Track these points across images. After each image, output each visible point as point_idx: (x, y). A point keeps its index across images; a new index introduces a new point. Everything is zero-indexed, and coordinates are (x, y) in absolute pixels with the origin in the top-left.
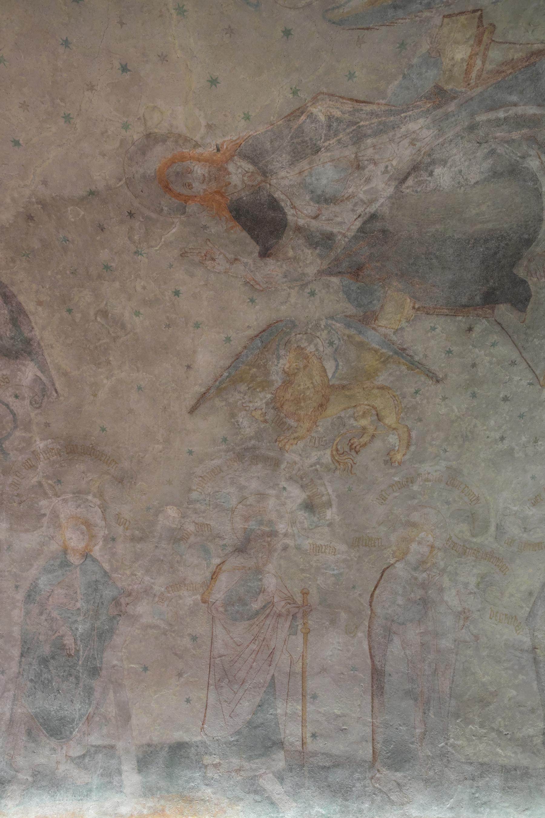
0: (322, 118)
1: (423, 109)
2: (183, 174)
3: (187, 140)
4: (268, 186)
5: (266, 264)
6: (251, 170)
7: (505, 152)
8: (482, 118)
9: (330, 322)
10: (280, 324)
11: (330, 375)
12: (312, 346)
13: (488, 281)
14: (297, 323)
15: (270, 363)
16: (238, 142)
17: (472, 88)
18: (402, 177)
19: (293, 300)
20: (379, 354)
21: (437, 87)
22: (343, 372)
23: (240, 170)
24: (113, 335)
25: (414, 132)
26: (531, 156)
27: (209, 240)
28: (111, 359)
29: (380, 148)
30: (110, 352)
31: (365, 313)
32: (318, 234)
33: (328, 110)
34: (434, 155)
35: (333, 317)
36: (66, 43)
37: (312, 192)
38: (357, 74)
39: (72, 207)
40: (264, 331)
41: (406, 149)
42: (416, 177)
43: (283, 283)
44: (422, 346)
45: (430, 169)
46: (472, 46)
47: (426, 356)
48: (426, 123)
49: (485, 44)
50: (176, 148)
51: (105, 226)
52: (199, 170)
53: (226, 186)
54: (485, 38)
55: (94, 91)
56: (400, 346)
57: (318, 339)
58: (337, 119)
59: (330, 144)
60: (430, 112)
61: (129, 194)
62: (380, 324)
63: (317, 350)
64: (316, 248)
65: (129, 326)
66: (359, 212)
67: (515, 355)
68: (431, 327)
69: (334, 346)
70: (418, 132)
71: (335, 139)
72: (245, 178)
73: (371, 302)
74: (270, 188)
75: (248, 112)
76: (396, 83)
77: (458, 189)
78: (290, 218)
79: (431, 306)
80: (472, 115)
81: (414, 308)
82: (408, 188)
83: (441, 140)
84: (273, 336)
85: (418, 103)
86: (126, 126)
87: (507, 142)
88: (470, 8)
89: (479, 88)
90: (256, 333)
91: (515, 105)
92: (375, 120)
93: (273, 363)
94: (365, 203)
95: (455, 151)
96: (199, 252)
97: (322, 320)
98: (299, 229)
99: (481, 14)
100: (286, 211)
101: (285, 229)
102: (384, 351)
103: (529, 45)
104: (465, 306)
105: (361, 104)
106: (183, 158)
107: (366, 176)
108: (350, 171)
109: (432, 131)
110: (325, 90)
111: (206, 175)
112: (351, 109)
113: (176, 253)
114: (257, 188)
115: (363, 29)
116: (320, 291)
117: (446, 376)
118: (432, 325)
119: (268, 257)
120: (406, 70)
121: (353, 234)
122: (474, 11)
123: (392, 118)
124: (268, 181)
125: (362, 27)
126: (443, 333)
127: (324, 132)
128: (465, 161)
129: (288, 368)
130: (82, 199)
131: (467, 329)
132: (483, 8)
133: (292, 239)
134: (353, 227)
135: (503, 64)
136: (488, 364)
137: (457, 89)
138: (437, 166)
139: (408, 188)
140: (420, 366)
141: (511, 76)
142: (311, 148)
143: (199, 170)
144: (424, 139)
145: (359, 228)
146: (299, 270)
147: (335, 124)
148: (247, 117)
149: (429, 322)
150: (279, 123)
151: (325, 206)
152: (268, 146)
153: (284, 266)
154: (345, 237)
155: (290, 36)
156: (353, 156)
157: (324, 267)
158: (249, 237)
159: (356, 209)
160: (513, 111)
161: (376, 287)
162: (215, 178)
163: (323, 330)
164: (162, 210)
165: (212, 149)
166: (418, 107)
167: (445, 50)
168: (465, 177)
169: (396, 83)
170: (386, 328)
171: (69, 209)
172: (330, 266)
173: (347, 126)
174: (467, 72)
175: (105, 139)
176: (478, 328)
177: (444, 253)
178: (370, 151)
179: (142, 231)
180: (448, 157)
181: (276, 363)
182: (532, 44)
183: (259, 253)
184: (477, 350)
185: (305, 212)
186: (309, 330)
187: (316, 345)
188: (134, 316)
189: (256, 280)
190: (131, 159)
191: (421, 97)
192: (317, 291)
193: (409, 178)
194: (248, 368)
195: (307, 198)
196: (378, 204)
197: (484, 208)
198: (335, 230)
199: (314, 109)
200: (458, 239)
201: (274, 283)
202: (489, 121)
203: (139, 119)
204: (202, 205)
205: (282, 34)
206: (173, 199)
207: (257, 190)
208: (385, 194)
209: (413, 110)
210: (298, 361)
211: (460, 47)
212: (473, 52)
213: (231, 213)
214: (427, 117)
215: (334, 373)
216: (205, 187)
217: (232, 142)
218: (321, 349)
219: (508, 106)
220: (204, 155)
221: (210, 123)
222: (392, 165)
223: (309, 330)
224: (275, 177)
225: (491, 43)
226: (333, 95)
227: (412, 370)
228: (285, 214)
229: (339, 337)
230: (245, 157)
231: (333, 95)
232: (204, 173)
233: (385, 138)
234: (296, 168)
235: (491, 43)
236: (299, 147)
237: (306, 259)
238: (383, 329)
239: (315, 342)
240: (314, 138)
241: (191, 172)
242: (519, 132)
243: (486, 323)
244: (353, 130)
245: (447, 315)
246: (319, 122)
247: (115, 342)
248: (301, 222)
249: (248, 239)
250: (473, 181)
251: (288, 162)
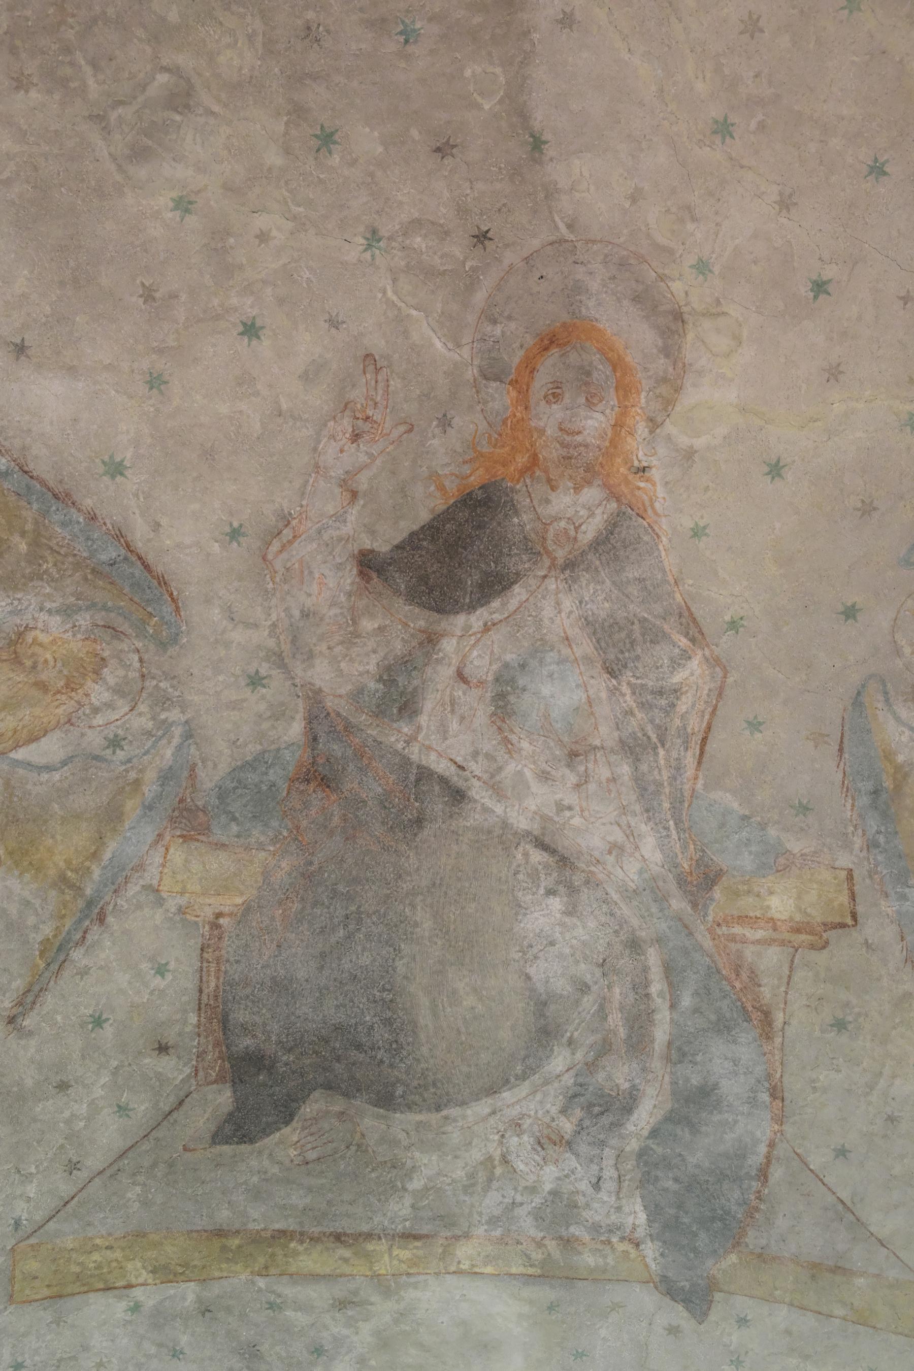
0: (677, 678)
1: (680, 856)
2: (587, 384)
3: (668, 404)
4: (542, 573)
5: (339, 567)
6: (580, 536)
7: (584, 1010)
8: (653, 958)
9: (178, 731)
10: (167, 609)
11: (20, 754)
12: (106, 696)
13: (290, 1050)
14: (172, 651)
15: (48, 590)
16: (650, 511)
17: (710, 931)
18: (547, 840)
19: (238, 635)
20: (87, 864)
21: (720, 874)
22: (29, 787)
23: (583, 512)
24: (113, 116)
25: (637, 847)
26: (573, 1054)
27: (410, 431)
28: (33, 94)
29: (610, 791)
30: (57, 97)
31: (204, 811)
32: (415, 682)
33: (691, 687)
34: (586, 890)
35: (191, 736)
36: (878, 170)
37: (523, 666)
38: (758, 736)
39: (502, 79)
40: (147, 567)
41: (603, 838)
42: (546, 866)
43: (287, 610)
44: (112, 957)
45: (561, 888)
46: (791, 919)
47: (84, 972)
48: (651, 866)
49: (792, 939)
50: (650, 377)
51: (448, 161)
52: (594, 424)
53: (549, 481)
54: (803, 937)
55: (777, 207)
56: (111, 907)
57: (127, 709)
58: (673, 705)
59: (624, 695)
60: (673, 869)
61: (536, 243)
62: (172, 851)
63: (96, 710)
64: (380, 680)
65: (141, 172)
66: (472, 766)
67: (94, 1162)
68: (167, 964)
69: (109, 751)
70: (637, 855)
71: (634, 705)
72: (563, 524)
73: (234, 819)
74: (535, 576)
75: (706, 535)
76: (735, 805)
77: (518, 948)
78: (461, 619)
79: (223, 952)
80: (659, 940)
81: (219, 915)
82: (526, 855)
83: (615, 896)
84: (133, 591)
85: (692, 847)
86: (702, 267)
87: (602, 1008)
88: (860, 909)
89: (711, 943)
90: (139, 545)
91: (673, 1007)
92: (665, 775)
93: (49, 596)
94: (492, 776)
95: (592, 924)
96: (376, 404)
97: (183, 712)
98: (430, 641)
99: (849, 926)
100: (478, 613)
101: (431, 609)
102: (96, 873)
103: (782, 1006)
104: (225, 1022)
105: (698, 747)
106: (625, 389)
107: (553, 773)
108: (566, 739)
109: (636, 878)
110: (730, 680)
111: (579, 438)
112: (689, 730)
113: (377, 344)
114: (539, 548)
115: (842, 742)
116: (263, 697)
117: (31, 1034)
118: (172, 966)
119: (361, 573)
120: (759, 819)
121: (414, 757)
122: (854, 916)
123: (666, 805)
124: (553, 573)
125: (845, 741)
126: (151, 993)
127: (651, 683)
128: (572, 947)
129: (35, 639)
130: (523, 115)
131: (164, 1042)
132: (858, 927)
133: (406, 625)
134: (433, 756)
135: (753, 972)
136: (67, 1114)
137: (711, 908)
138: (565, 899)
139: (526, 855)
140: (54, 967)
141: (728, 988)
142: (618, 660)
143: (594, 424)
144: (622, 868)
145: (430, 769)
146: (323, 647)
147: (663, 702)
148: (697, 532)
149: (182, 958)
150: (678, 596)
151: (489, 694)
152: (632, 573)
153: (335, 611)
154: (408, 742)
155: (843, 617)
156: (597, 742)
157: (329, 703)
158: (415, 527)
159: (480, 758)
160: (661, 1005)
161: (275, 823)
162: (570, 458)
163: (153, 718)
164: (495, 322)
165: (641, 457)
166: (685, 847)
167: (789, 878)
168: (541, 954)
169: (735, 805)
170: (164, 866)
171: (498, 70)
172: (332, 715)
173: (657, 725)
174: (742, 919)
175: (674, 210)
176: (167, 1065)
177: (359, 948)
178: (604, 773)
179: (437, 260)
180: (581, 914)
181: (48, 605)
182: (784, 1010)
183: (372, 551)
184: (105, 1079)
185: (475, 653)
186: (154, 682)
187: (110, 705)
188: (175, 194)
189: (296, 544)
190: (623, 264)
191: (703, 851)
192: (264, 690)
193: (545, 854)
194: (29, 527)
195: (508, 657)
196: (489, 803)
197: (469, 1001)
198: (423, 719)
199: (697, 662)
200: (394, 970)
201: (286, 587)
202: (646, 969)
203: (718, 302)
204: (504, 422)
205: (849, 604)
206: (521, 353)
207: (534, 549)
208: (515, 814)
209: (679, 840)
210: (59, 664)
211: (791, 901)
212: (779, 923)
213: (480, 488)
214: (663, 866)
215: (28, 765)
216: (549, 432)
217: (651, 500)
218: (99, 720)
219: (671, 995)
220: (629, 439)
221: (696, 457)
222: (572, 817)
223: (154, 682)
224: (561, 587)
225: (794, 947)
226: (720, 695)
227: (42, 953)
228: (472, 608)
229: (135, 760)
230: (613, 526)
231: (720, 695)
232: (585, 433)
233: (630, 797)
234: (577, 630)
235: (794, 947)
236: (623, 635)
237: (352, 660)
238: (158, 860)
239: (120, 702)
240: (639, 665)
241: (590, 404)
242: (620, 1024)
243: (181, 1077)
244: (649, 738)
245: (201, 991)
246: (672, 673)
247: (91, 117)
248: (448, 646)
249: (407, 527)
250: (532, 971)
251: (593, 614)
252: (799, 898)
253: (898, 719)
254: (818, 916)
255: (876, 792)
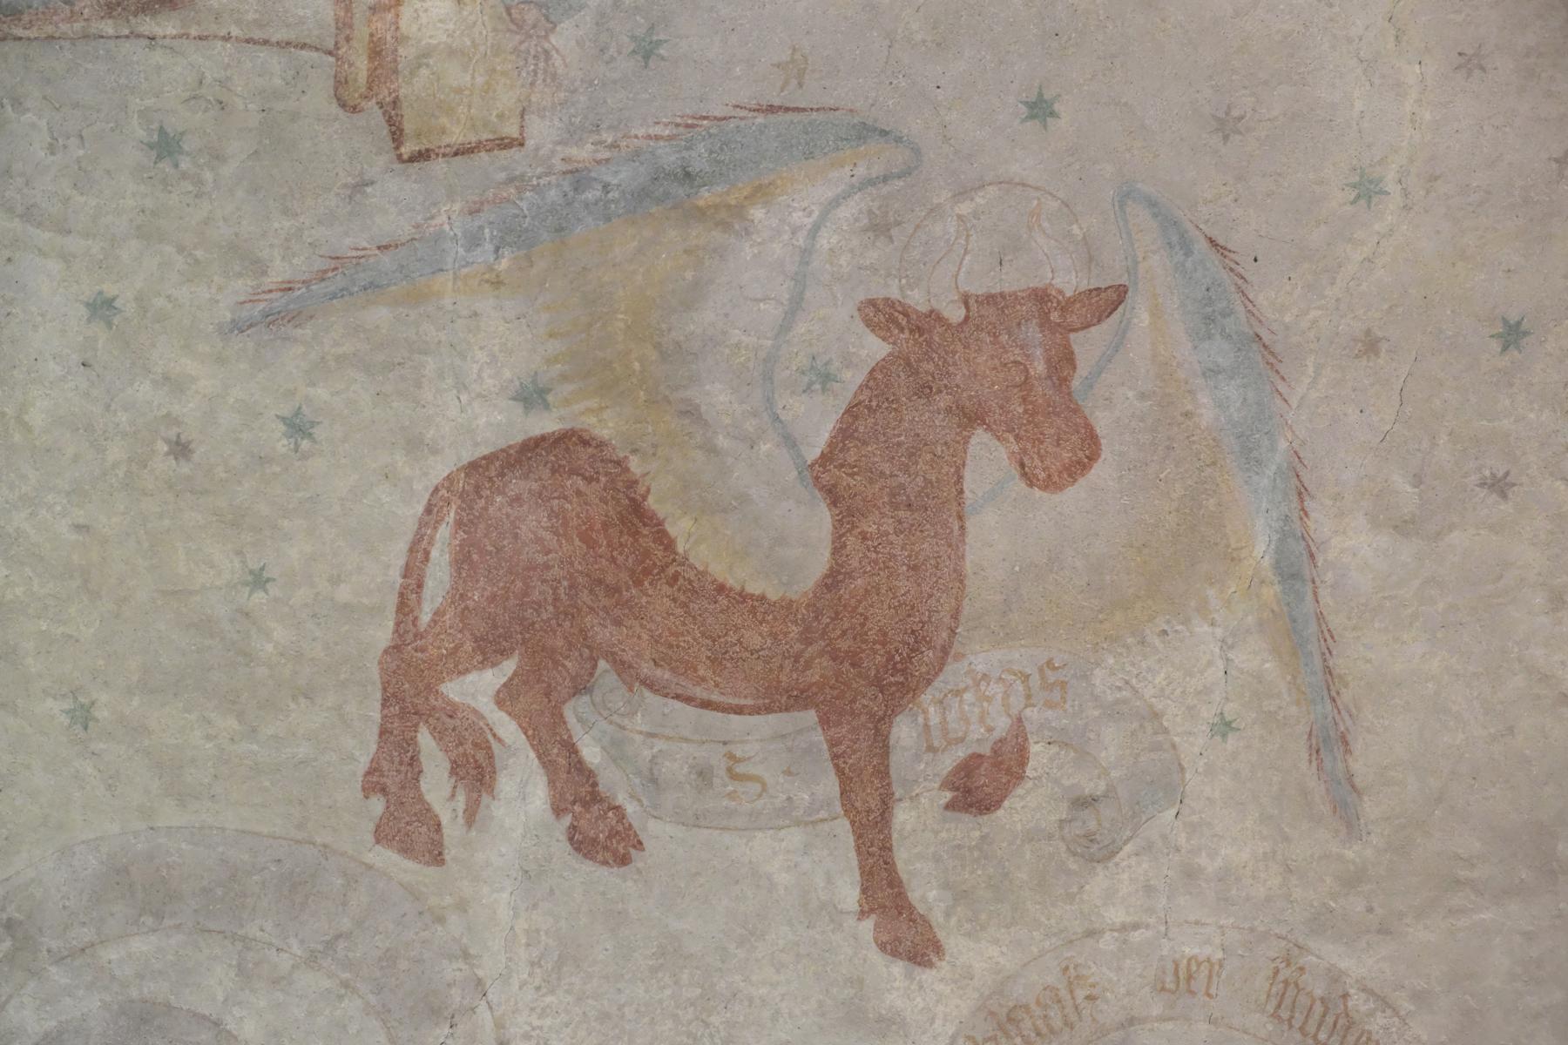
46: (400, 40)
49: (354, 43)
88: (439, 167)
99: (397, 148)
103: (194, 32)
115: (787, 109)
122: (422, 156)
125: (789, 116)
132: (398, 166)
167: (495, 30)
205: (1056, 107)
211: (444, 38)
212: (390, 16)
252: (452, 52)
253: (835, 203)
254: (413, 88)
255: (688, 176)
